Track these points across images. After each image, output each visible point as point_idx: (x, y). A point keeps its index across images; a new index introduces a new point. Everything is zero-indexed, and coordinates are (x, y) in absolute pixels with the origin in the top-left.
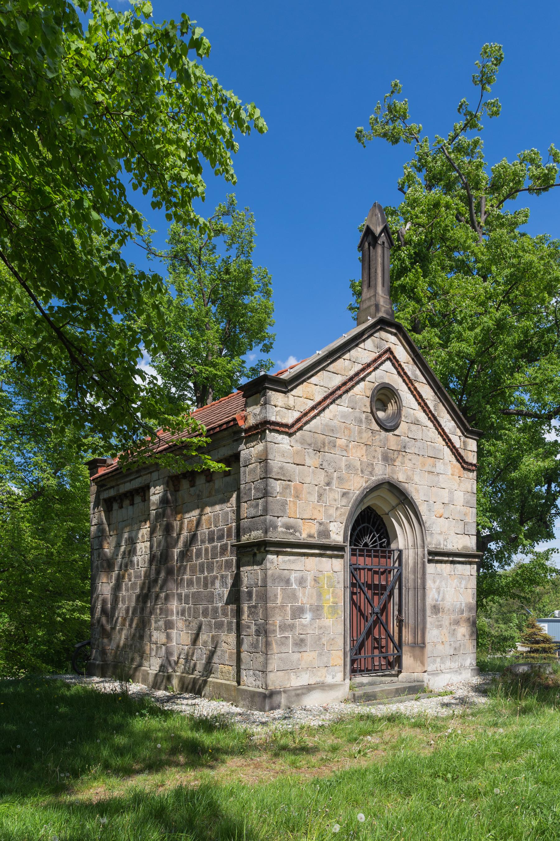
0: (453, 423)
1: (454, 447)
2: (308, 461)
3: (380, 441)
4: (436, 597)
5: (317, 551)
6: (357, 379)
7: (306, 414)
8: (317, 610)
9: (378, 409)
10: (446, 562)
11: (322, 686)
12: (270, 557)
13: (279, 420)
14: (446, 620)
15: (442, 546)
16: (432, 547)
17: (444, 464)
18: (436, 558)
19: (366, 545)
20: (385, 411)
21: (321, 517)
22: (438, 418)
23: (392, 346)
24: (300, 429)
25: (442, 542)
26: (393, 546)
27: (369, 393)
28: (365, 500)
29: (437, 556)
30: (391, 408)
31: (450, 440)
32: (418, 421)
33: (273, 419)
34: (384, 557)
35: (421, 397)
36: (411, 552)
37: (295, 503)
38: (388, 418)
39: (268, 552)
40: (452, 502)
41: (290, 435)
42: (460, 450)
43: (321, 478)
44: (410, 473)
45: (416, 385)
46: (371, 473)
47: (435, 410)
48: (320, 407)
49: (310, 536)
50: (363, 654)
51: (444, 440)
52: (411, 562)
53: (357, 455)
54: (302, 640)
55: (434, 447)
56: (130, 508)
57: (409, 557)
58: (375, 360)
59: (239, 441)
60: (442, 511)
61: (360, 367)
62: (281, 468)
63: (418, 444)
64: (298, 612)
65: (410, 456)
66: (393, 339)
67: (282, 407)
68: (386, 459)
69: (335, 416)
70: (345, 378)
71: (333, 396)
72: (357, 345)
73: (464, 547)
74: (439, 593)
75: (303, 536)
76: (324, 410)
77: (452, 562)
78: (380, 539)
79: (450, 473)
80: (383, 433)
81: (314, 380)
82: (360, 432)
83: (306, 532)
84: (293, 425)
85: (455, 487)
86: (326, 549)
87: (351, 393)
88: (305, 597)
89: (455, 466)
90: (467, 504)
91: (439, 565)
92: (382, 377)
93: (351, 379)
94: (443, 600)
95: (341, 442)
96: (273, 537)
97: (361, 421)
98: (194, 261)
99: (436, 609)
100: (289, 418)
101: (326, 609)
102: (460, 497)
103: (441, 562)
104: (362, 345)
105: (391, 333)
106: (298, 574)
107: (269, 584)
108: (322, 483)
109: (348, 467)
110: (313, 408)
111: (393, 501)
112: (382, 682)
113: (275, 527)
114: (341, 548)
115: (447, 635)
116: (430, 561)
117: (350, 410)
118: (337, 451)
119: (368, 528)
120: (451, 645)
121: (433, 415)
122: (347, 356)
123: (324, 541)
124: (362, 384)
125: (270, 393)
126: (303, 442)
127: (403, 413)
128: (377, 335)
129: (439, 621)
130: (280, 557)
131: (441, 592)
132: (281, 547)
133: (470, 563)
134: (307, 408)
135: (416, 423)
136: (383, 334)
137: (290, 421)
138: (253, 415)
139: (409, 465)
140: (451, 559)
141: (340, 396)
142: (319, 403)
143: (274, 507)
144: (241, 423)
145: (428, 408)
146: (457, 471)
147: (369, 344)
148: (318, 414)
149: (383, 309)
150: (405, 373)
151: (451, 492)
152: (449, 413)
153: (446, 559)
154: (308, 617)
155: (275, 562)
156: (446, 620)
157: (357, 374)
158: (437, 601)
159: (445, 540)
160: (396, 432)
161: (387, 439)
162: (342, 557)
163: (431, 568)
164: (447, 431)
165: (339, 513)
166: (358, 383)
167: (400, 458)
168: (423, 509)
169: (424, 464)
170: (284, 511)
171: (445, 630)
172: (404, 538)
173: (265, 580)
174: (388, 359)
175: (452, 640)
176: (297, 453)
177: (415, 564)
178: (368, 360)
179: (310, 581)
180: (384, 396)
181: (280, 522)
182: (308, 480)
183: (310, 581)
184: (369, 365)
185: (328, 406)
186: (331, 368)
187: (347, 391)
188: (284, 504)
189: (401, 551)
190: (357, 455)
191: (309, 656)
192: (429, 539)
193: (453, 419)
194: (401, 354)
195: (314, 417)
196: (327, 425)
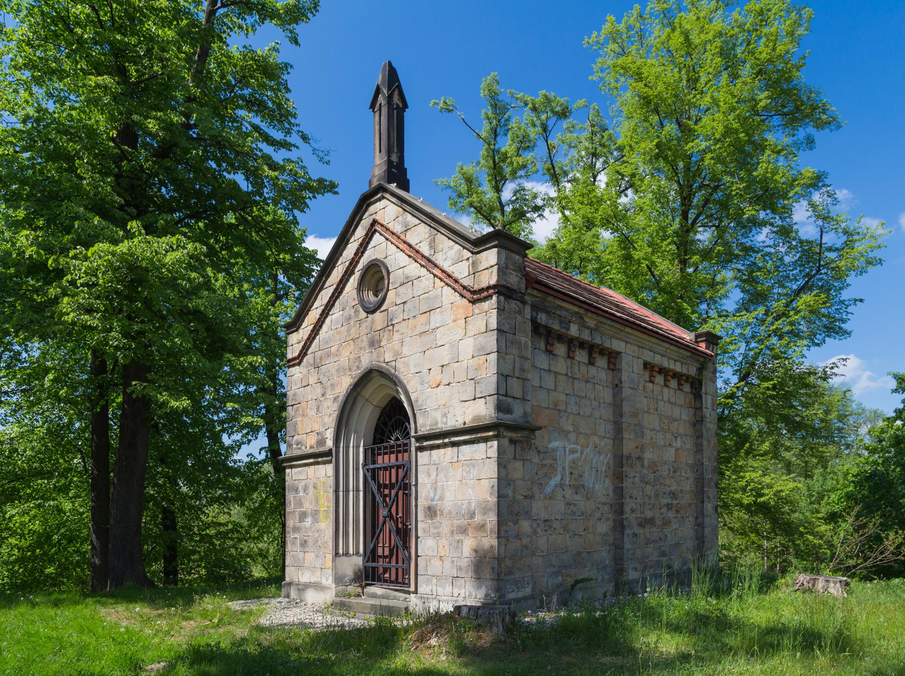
0: (457, 247)
3: (366, 328)
4: (432, 495)
5: (312, 460)
8: (315, 513)
10: (445, 446)
11: (317, 586)
14: (445, 525)
15: (440, 425)
17: (441, 313)
18: (425, 444)
21: (317, 427)
23: (378, 217)
25: (439, 421)
32: (407, 278)
35: (410, 246)
43: (319, 391)
44: (397, 347)
50: (393, 563)
51: (441, 280)
54: (306, 541)
55: (428, 298)
60: (438, 378)
64: (303, 516)
72: (347, 244)
73: (475, 419)
74: (436, 489)
82: (349, 330)
85: (461, 332)
86: (319, 457)
92: (370, 256)
94: (441, 498)
99: (431, 512)
101: (321, 515)
102: (468, 347)
103: (438, 447)
108: (320, 395)
109: (338, 371)
112: (395, 598)
115: (447, 547)
117: (341, 313)
119: (400, 419)
120: (453, 562)
123: (322, 449)
129: (436, 528)
131: (439, 488)
133: (486, 440)
135: (408, 281)
136: (372, 209)
139: (397, 336)
140: (447, 440)
145: (417, 252)
152: (449, 238)
153: (440, 441)
154: (309, 520)
158: (433, 500)
159: (445, 415)
160: (382, 309)
161: (373, 322)
162: (330, 462)
163: (423, 457)
164: (446, 266)
170: (295, 431)
171: (444, 540)
175: (455, 555)
179: (311, 489)
191: (310, 557)
193: (456, 243)
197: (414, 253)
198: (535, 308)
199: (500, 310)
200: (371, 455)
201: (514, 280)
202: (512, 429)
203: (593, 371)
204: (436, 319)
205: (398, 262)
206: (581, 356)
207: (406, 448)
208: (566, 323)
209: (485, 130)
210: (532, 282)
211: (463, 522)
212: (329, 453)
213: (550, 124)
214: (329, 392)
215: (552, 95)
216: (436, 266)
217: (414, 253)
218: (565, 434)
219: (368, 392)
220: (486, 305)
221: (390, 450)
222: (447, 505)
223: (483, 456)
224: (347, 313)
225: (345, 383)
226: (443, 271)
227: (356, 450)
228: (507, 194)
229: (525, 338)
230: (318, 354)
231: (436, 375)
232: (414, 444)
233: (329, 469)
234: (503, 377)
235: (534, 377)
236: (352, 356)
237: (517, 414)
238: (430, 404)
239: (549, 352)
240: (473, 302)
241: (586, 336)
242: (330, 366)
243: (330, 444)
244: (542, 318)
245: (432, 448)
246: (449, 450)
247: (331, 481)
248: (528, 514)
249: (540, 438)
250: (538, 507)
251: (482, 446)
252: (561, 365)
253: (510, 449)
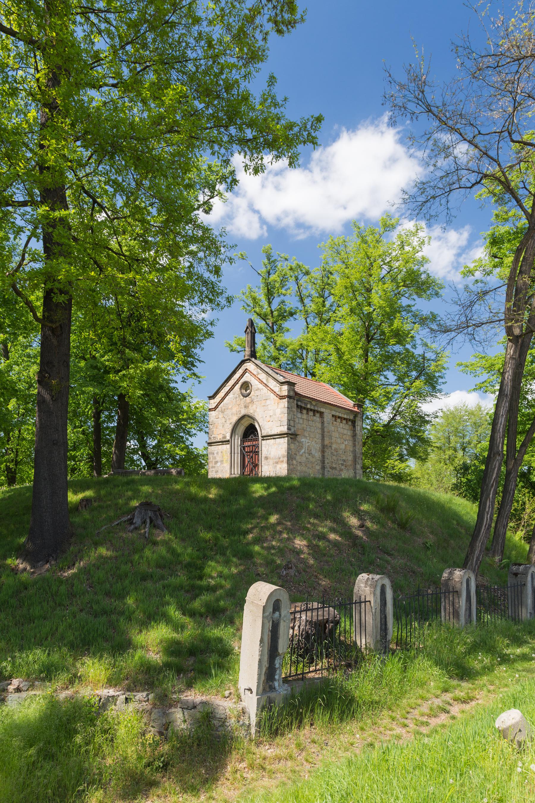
14: (271, 462)
43: (224, 420)
75: (219, 440)
83: (219, 438)
86: (223, 442)
88: (218, 459)
90: (282, 413)
102: (278, 411)
139: (254, 406)
156: (271, 462)
163: (264, 442)
183: (220, 453)
198: (297, 401)
199: (288, 402)
200: (243, 441)
201: (292, 394)
202: (292, 435)
203: (315, 418)
204: (268, 402)
205: (255, 383)
206: (311, 413)
207: (257, 440)
208: (306, 404)
209: (263, 270)
210: (296, 394)
211: (277, 460)
212: (228, 441)
213: (300, 277)
215: (301, 263)
218: (306, 437)
219: (242, 422)
220: (284, 400)
221: (251, 440)
222: (272, 456)
223: (283, 442)
225: (235, 419)
227: (237, 440)
228: (275, 305)
229: (295, 409)
230: (223, 408)
231: (268, 418)
232: (260, 438)
233: (228, 446)
234: (289, 420)
235: (297, 420)
237: (292, 431)
239: (301, 413)
241: (312, 408)
242: (228, 412)
243: (228, 438)
244: (299, 403)
247: (229, 450)
248: (295, 459)
249: (299, 438)
250: (298, 458)
252: (305, 416)
253: (291, 440)
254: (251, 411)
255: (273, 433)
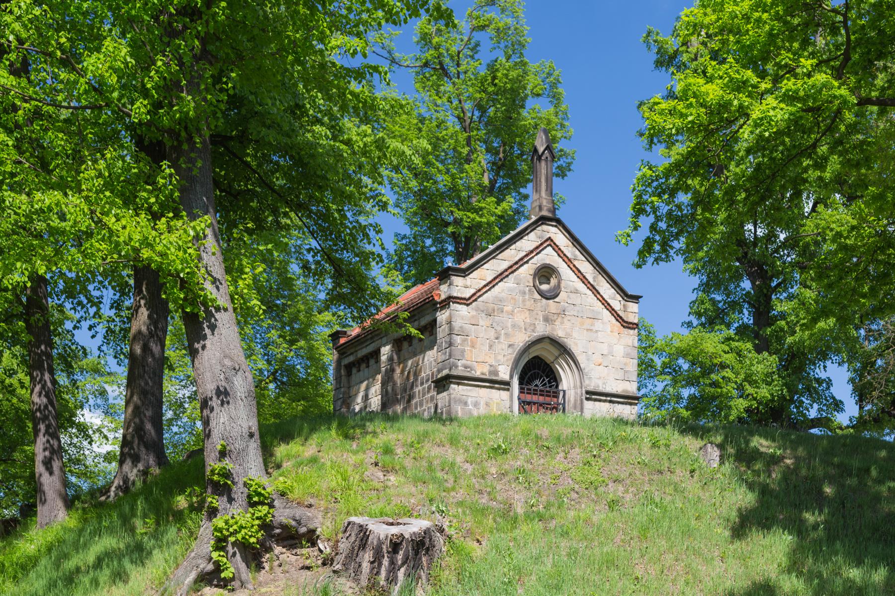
1: (613, 310)
2: (481, 323)
6: (521, 263)
7: (479, 290)
9: (541, 283)
10: (605, 401)
12: (452, 386)
13: (459, 295)
16: (591, 388)
19: (536, 385)
20: (549, 284)
22: (597, 287)
24: (476, 300)
25: (601, 385)
26: (560, 388)
27: (532, 272)
28: (531, 350)
29: (593, 395)
30: (553, 281)
31: (609, 304)
33: (455, 295)
34: (554, 397)
35: (579, 271)
36: (572, 392)
37: (471, 351)
38: (549, 291)
39: (451, 383)
40: (611, 353)
41: (468, 305)
42: (619, 312)
43: (492, 334)
45: (576, 263)
46: (533, 331)
47: (594, 281)
48: (491, 284)
49: (483, 374)
52: (572, 399)
53: (521, 318)
56: (366, 370)
57: (571, 396)
58: (537, 248)
59: (436, 310)
60: (600, 361)
61: (524, 253)
62: (461, 327)
63: (576, 308)
65: (569, 318)
66: (554, 229)
67: (461, 286)
68: (546, 319)
69: (503, 290)
70: (511, 263)
71: (501, 277)
72: (522, 238)
73: (623, 391)
75: (478, 374)
76: (494, 286)
77: (610, 402)
78: (549, 382)
79: (609, 330)
80: (544, 301)
81: (485, 266)
82: (524, 301)
84: (470, 298)
87: (515, 274)
89: (614, 325)
90: (627, 355)
91: (597, 403)
93: (516, 263)
95: (508, 308)
96: (454, 372)
97: (524, 293)
98: (453, 70)
100: (467, 294)
103: (600, 401)
104: (526, 238)
105: (552, 226)
106: (474, 399)
107: (452, 404)
108: (493, 338)
109: (514, 326)
110: (485, 286)
111: (556, 353)
113: (457, 367)
114: (507, 384)
116: (587, 399)
118: (504, 315)
121: (592, 285)
122: (513, 247)
124: (526, 266)
125: (453, 278)
126: (477, 309)
127: (562, 285)
128: (539, 228)
130: (460, 387)
132: (461, 380)
134: (481, 286)
135: (576, 292)
136: (545, 227)
137: (467, 296)
138: (444, 291)
139: (567, 325)
141: (507, 276)
142: (490, 282)
143: (456, 354)
144: (436, 298)
146: (616, 329)
147: (532, 236)
148: (489, 290)
149: (545, 208)
150: (565, 255)
151: (610, 346)
155: (456, 390)
157: (521, 259)
159: (604, 383)
160: (556, 300)
162: (508, 390)
165: (505, 358)
166: (522, 265)
167: (559, 319)
168: (581, 358)
169: (582, 324)
170: (463, 356)
172: (567, 381)
173: (449, 402)
174: (550, 245)
176: (473, 317)
177: (576, 401)
178: (531, 248)
180: (545, 273)
181: (460, 363)
182: (481, 335)
184: (532, 252)
185: (497, 284)
186: (500, 257)
187: (512, 272)
188: (463, 351)
189: (564, 391)
190: (521, 318)
192: (587, 382)
194: (561, 239)
195: (486, 292)
196: (496, 297)
197: (583, 279)
204: (598, 325)
214: (502, 338)
216: (599, 293)
217: (583, 279)
220: (632, 332)
224: (522, 287)
226: (603, 299)
231: (597, 358)
233: (504, 395)
236: (528, 320)
238: (593, 375)
240: (624, 327)
245: (596, 400)
246: (607, 404)
251: (628, 407)
254: (559, 332)
255: (608, 390)
